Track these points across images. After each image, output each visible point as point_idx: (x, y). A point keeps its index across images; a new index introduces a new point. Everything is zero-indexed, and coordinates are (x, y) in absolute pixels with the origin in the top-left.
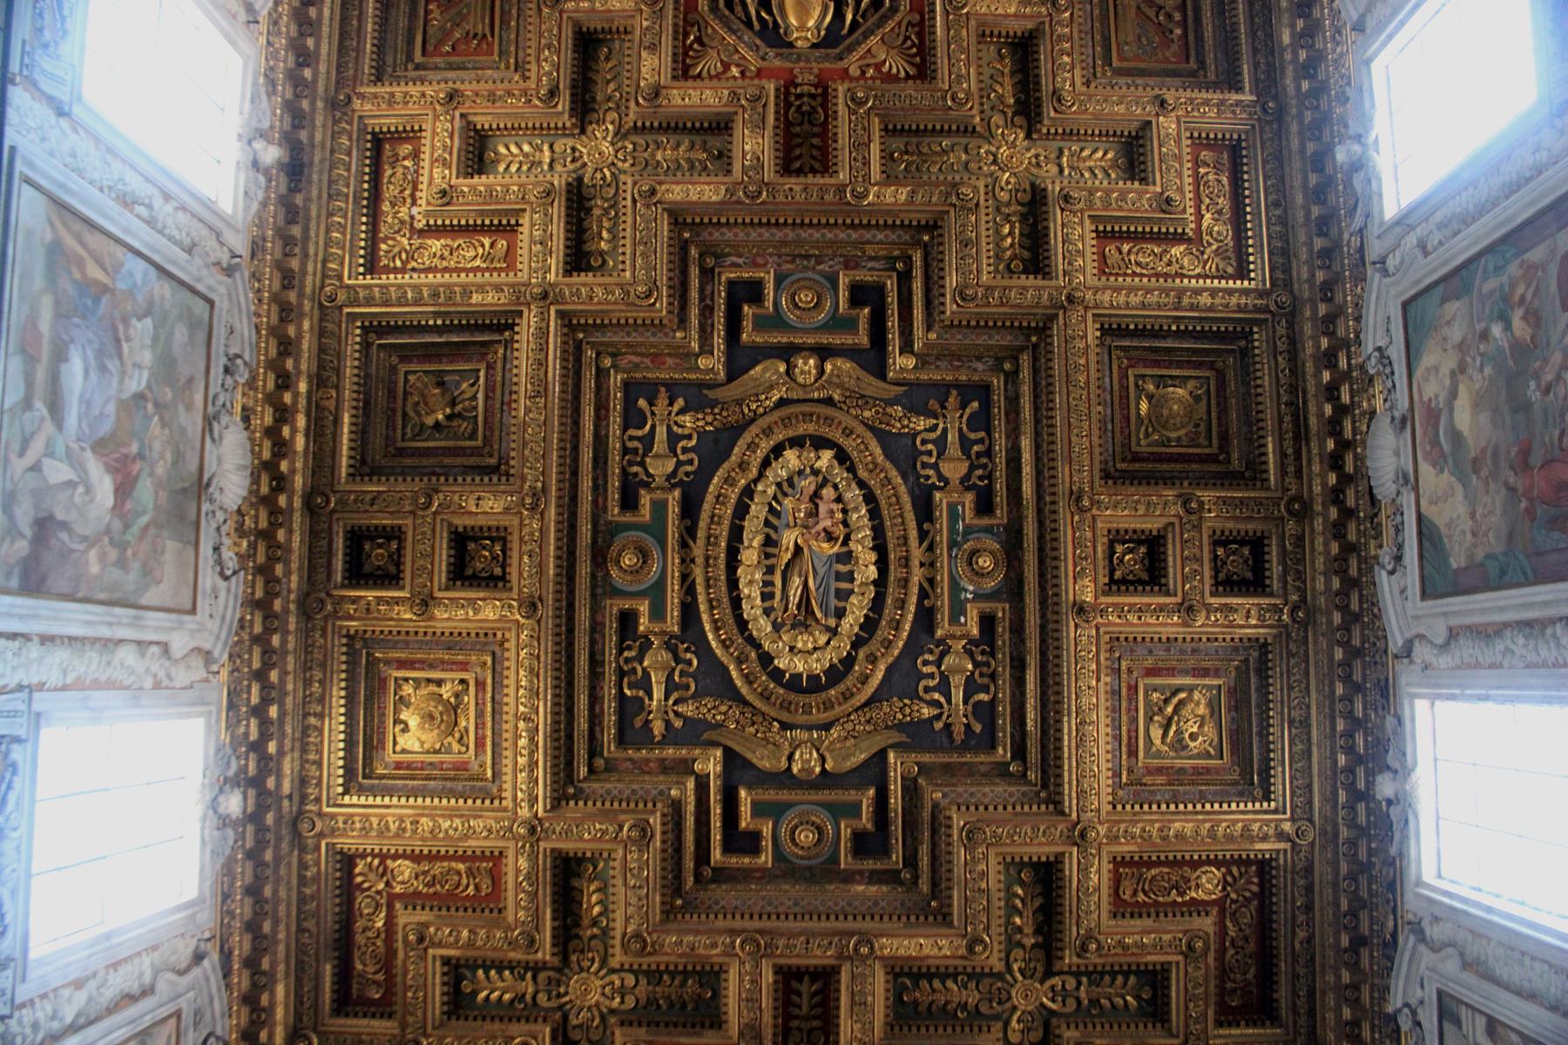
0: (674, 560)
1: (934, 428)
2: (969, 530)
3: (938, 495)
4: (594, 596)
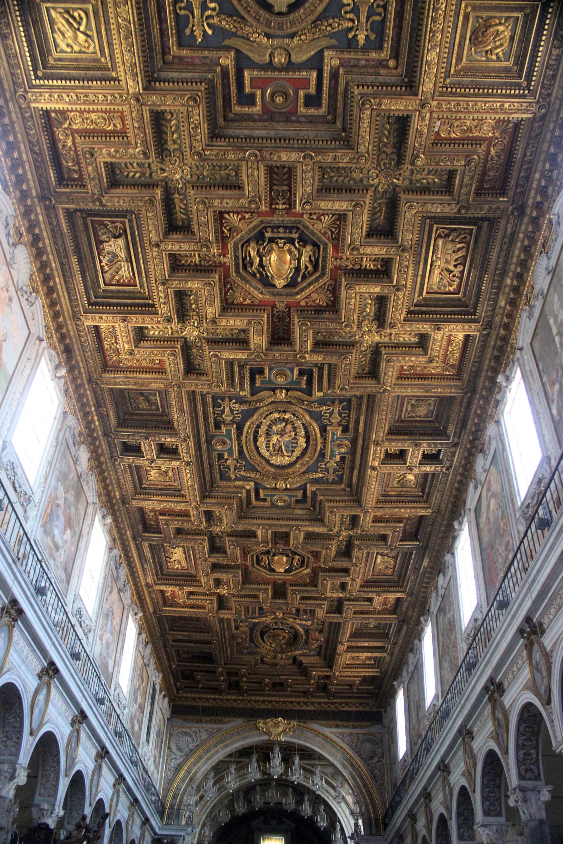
0: (235, 443)
1: (329, 409)
2: (338, 439)
3: (328, 428)
4: (208, 451)
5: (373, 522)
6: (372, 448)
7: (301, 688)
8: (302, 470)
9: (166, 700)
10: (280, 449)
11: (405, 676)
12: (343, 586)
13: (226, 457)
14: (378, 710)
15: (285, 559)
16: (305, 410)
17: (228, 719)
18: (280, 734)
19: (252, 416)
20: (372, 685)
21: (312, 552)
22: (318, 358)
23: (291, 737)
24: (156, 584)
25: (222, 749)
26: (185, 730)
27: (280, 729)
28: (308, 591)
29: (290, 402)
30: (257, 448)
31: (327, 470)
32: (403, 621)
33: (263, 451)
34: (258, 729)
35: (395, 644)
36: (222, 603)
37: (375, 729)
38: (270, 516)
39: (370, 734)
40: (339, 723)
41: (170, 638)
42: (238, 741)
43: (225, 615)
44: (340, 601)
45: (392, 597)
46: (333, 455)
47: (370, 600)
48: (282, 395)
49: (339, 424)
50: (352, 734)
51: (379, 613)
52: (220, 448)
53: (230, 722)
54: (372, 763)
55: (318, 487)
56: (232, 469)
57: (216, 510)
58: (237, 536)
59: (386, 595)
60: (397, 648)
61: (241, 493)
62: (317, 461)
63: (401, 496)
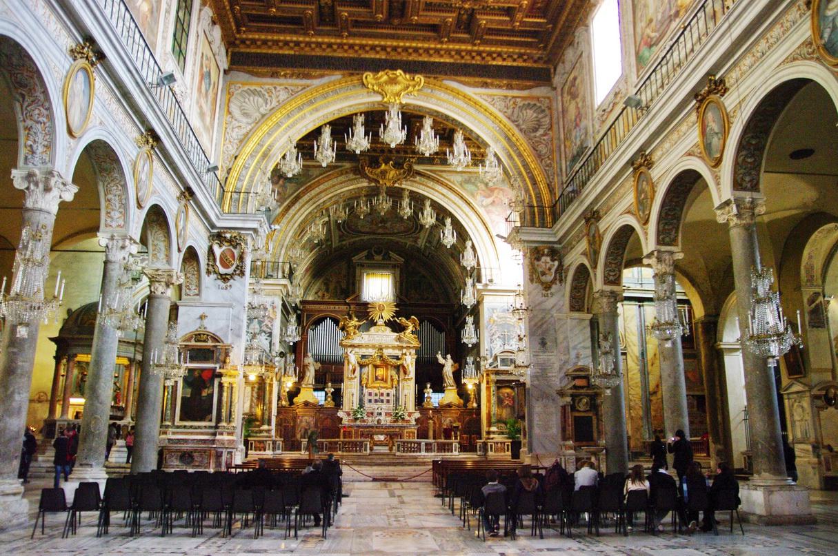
14: (545, 66)
17: (318, 72)
18: (398, 94)
20: (544, 17)
25: (311, 114)
26: (252, 88)
39: (532, 98)
40: (489, 81)
42: (335, 102)
50: (506, 97)
53: (322, 76)
54: (535, 137)
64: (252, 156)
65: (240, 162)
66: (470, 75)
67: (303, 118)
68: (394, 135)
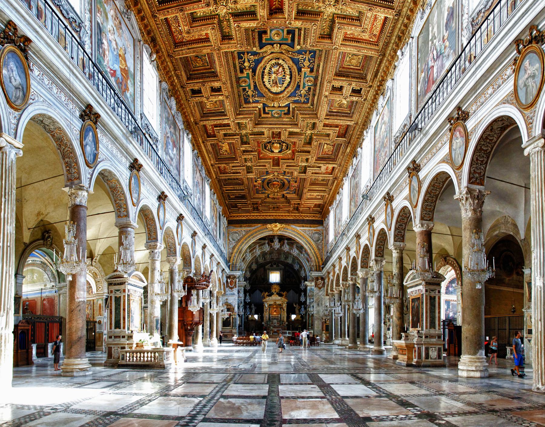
5: (324, 126)
6: (325, 83)
7: (287, 209)
8: (288, 95)
9: (225, 218)
10: (276, 83)
11: (334, 205)
12: (307, 160)
13: (247, 90)
15: (278, 145)
16: (290, 57)
19: (261, 62)
21: (292, 142)
22: (298, 24)
23: (283, 231)
24: (216, 164)
27: (277, 228)
28: (290, 163)
29: (282, 53)
30: (264, 82)
31: (301, 95)
32: (335, 178)
33: (267, 83)
34: (267, 228)
35: (331, 189)
36: (249, 170)
37: (320, 228)
38: (271, 122)
41: (224, 189)
43: (251, 176)
44: (305, 167)
45: (330, 166)
46: (304, 87)
47: (320, 167)
48: (277, 48)
49: (308, 67)
51: (324, 174)
52: (244, 85)
55: (296, 105)
56: (251, 96)
57: (244, 121)
58: (255, 135)
59: (327, 165)
60: (332, 191)
61: (256, 110)
62: (296, 90)
63: (339, 112)
64: (236, 253)
65: (233, 255)
66: (298, 223)
67: (250, 240)
68: (276, 245)
